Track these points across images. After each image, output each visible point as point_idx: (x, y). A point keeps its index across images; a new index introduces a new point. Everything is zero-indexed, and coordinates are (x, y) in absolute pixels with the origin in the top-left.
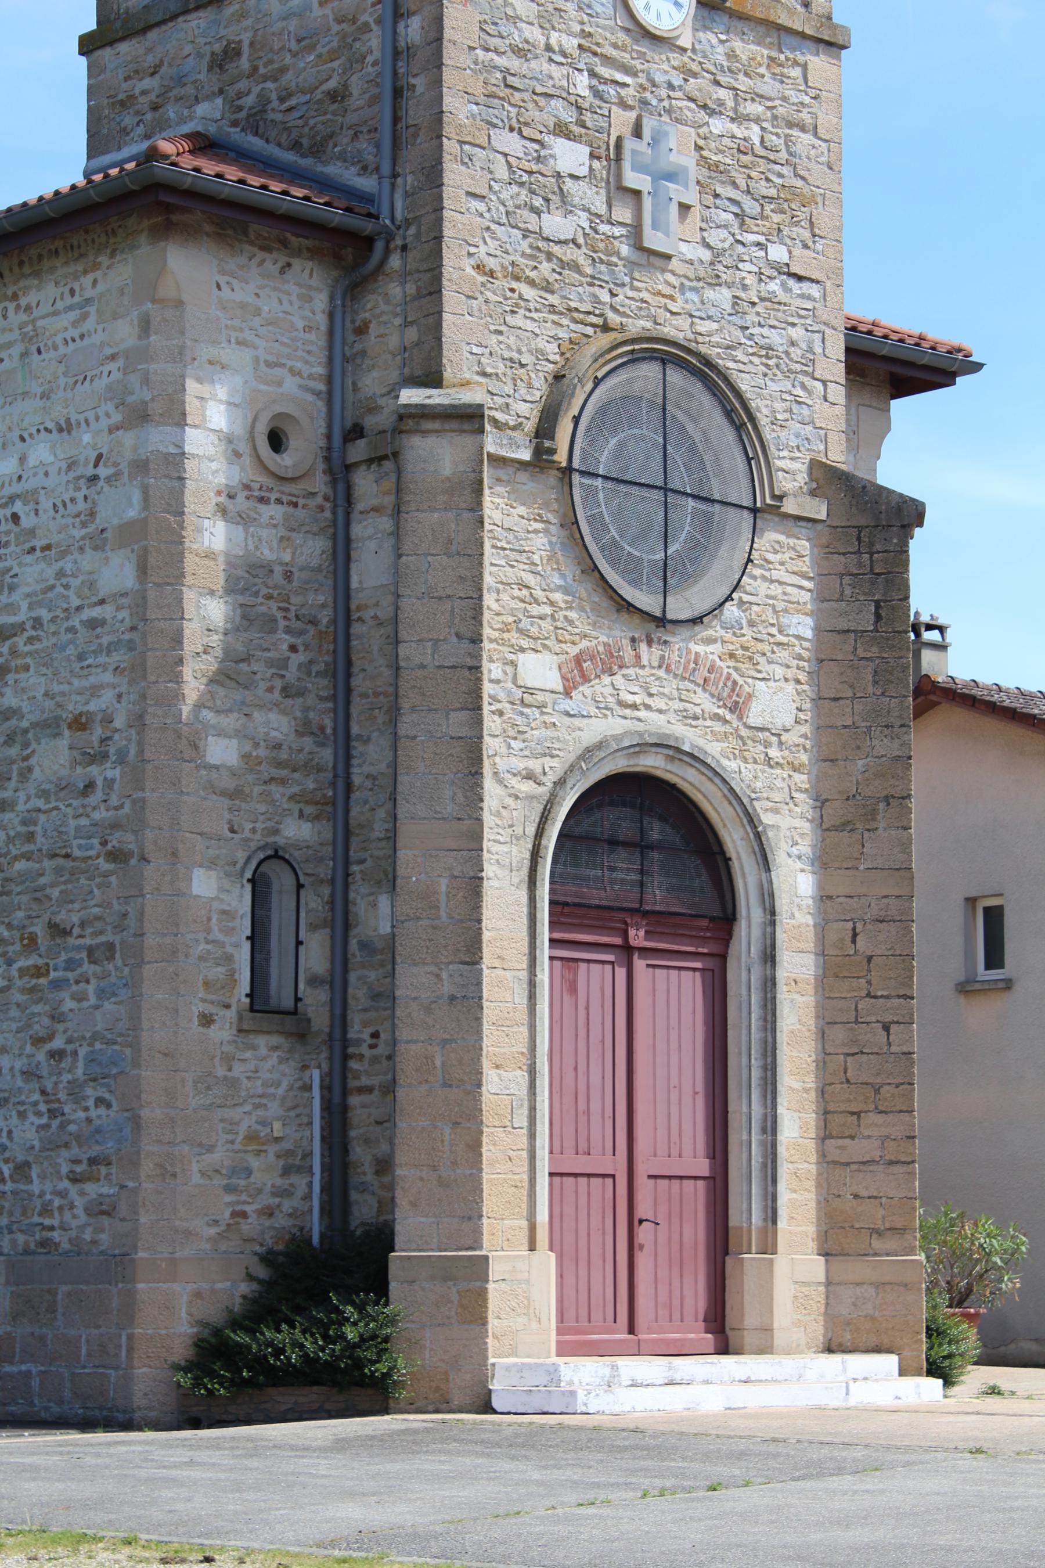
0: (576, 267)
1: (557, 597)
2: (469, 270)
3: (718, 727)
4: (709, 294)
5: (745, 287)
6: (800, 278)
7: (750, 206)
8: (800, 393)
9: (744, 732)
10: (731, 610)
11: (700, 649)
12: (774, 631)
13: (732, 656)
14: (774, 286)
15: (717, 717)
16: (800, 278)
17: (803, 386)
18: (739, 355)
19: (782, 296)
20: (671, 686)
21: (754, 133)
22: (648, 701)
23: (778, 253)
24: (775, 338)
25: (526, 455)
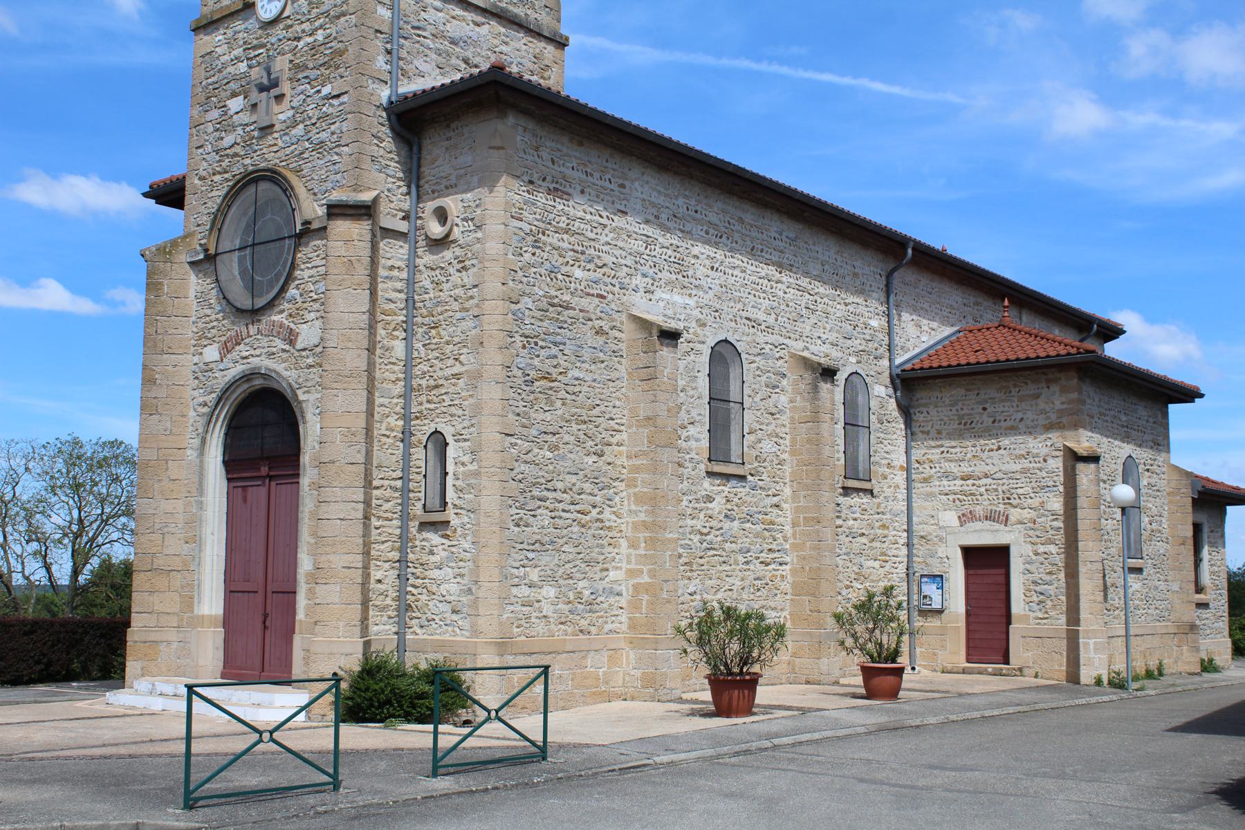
0: (236, 155)
1: (220, 316)
2: (197, 181)
3: (285, 355)
4: (294, 132)
5: (310, 118)
6: (338, 96)
7: (313, 74)
8: (336, 157)
9: (297, 354)
10: (292, 292)
11: (276, 318)
12: (312, 294)
13: (291, 315)
14: (324, 109)
15: (284, 350)
16: (338, 96)
17: (337, 154)
18: (305, 156)
19: (331, 110)
20: (264, 341)
21: (320, 36)
22: (252, 352)
23: (326, 90)
24: (323, 135)
25: (201, 256)
